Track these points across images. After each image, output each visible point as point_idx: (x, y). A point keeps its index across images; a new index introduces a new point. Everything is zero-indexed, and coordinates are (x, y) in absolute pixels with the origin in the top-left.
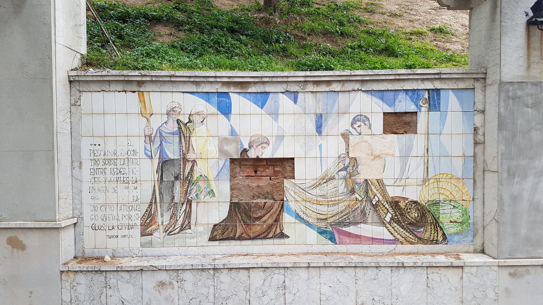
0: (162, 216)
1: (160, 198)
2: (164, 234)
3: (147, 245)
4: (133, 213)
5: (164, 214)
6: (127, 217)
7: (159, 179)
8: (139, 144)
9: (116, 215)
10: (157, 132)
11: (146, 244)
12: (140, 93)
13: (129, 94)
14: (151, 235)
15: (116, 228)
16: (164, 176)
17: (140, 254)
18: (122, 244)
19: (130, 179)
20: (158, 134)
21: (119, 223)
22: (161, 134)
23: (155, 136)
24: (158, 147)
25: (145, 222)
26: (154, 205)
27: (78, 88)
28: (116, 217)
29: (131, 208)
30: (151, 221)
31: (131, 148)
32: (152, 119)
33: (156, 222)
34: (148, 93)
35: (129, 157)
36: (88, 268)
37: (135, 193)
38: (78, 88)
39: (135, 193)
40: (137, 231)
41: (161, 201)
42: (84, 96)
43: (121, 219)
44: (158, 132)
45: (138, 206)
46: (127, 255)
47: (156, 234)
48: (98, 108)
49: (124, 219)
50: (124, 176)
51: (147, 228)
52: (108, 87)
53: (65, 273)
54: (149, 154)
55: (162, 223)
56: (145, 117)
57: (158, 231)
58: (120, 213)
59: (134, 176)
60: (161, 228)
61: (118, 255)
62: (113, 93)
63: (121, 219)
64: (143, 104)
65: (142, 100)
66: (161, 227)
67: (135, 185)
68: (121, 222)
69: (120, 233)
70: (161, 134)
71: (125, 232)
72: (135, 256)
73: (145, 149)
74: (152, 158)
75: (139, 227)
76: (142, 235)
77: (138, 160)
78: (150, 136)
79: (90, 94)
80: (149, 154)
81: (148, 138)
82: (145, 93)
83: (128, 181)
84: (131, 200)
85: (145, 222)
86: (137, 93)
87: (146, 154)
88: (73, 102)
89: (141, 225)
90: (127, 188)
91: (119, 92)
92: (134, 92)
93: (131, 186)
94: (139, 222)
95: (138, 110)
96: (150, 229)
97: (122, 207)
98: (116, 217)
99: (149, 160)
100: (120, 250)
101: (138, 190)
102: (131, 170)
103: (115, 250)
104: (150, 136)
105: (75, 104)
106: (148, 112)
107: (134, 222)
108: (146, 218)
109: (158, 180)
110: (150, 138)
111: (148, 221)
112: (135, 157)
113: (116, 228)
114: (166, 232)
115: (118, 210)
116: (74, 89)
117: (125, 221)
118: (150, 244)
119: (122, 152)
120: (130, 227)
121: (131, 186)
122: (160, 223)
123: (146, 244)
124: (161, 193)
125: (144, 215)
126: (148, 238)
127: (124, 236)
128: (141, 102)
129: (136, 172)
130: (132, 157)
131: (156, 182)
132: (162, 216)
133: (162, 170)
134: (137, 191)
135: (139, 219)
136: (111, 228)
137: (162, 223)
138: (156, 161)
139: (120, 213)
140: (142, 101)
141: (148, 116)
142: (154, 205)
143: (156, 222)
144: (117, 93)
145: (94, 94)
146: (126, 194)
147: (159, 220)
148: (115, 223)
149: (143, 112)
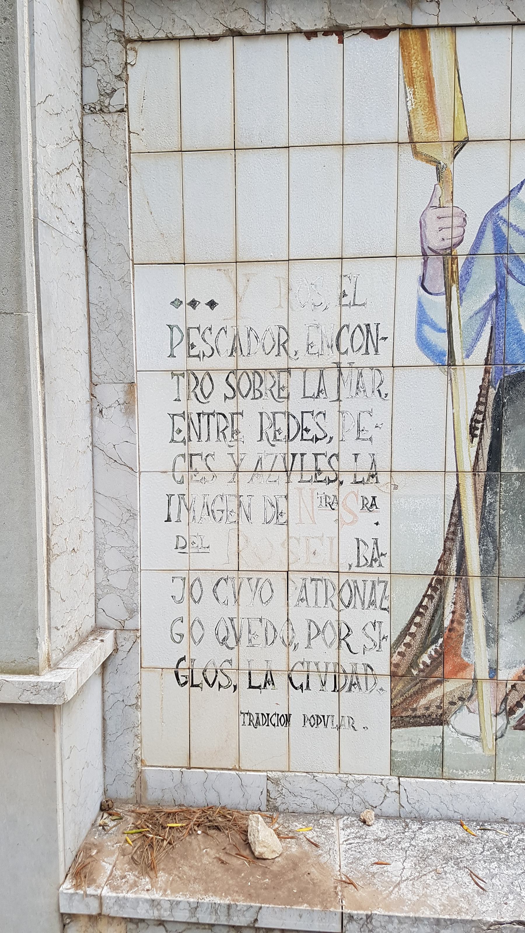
0: (492, 637)
1: (484, 553)
2: (501, 721)
3: (422, 767)
4: (356, 617)
5: (503, 629)
6: (330, 634)
7: (483, 465)
8: (393, 296)
9: (281, 626)
10: (481, 232)
11: (415, 762)
12: (412, 37)
13: (359, 45)
14: (440, 721)
15: (281, 680)
16: (504, 450)
17: (390, 807)
18: (307, 757)
19: (346, 462)
20: (488, 245)
21: (295, 657)
22: (500, 240)
23: (473, 253)
24: (486, 308)
25: (413, 664)
26: (452, 585)
27: (117, 23)
28: (282, 632)
29: (348, 594)
30: (439, 659)
31: (354, 317)
32: (463, 166)
33: (464, 667)
34: (447, 35)
35: (345, 361)
36: (195, 908)
37: (364, 526)
38: (117, 23)
39: (364, 526)
40: (374, 703)
41: (486, 569)
42: (150, 67)
43: (301, 638)
44: (489, 235)
45: (380, 588)
46: (331, 807)
47: (463, 721)
48: (207, 123)
49: (317, 643)
50: (321, 447)
51: (422, 692)
52: (256, 11)
53: (83, 922)
54: (441, 341)
55: (493, 671)
56: (430, 160)
57: (473, 705)
58: (300, 615)
59: (364, 449)
60: (488, 696)
61: (292, 803)
62: (280, 43)
63: (301, 638)
64: (421, 94)
65: (418, 72)
66: (486, 689)
67: (368, 490)
68: (301, 654)
69: (302, 704)
70: (500, 240)
71: (320, 700)
72: (369, 815)
73: (423, 319)
74: (452, 363)
75: (385, 683)
76: (402, 717)
77: (387, 373)
78: (448, 255)
79: (169, 51)
80: (441, 341)
81: (436, 265)
82: (433, 37)
83: (337, 473)
84: (349, 555)
85: (413, 664)
86: (393, 38)
87: (424, 344)
88: (92, 96)
89: (393, 675)
90: (332, 504)
91: (310, 35)
92: (380, 33)
93: (351, 495)
94: (382, 662)
95: (393, 127)
96: (435, 694)
97: (311, 587)
98: (282, 632)
99: (438, 376)
100: (301, 783)
101: (382, 513)
102: (350, 423)
103: (276, 782)
104: (448, 255)
105: (102, 104)
106: (446, 131)
107: (361, 659)
108: (416, 643)
109: (475, 471)
110: (446, 266)
111: (425, 658)
112: (372, 360)
113: (281, 680)
114: (511, 712)
115: (293, 601)
116: (97, 33)
117: (323, 654)
118: (437, 763)
119: (316, 338)
120: (342, 681)
121: (351, 495)
122: (483, 673)
123: (415, 762)
124: (486, 532)
125: (406, 631)
126: (427, 736)
127: (319, 720)
128: (411, 81)
129: (372, 432)
130: (359, 359)
131: (468, 482)
132: (492, 637)
133: (498, 422)
134: (373, 517)
135: (386, 645)
136: (258, 680)
137: (493, 671)
138: (471, 379)
139: (300, 615)
140: (418, 78)
141: (443, 154)
142: (452, 585)
143: (464, 667)
144: (298, 42)
145: (191, 52)
146: (322, 532)
147: (477, 654)
148: (277, 659)
149: (421, 131)
